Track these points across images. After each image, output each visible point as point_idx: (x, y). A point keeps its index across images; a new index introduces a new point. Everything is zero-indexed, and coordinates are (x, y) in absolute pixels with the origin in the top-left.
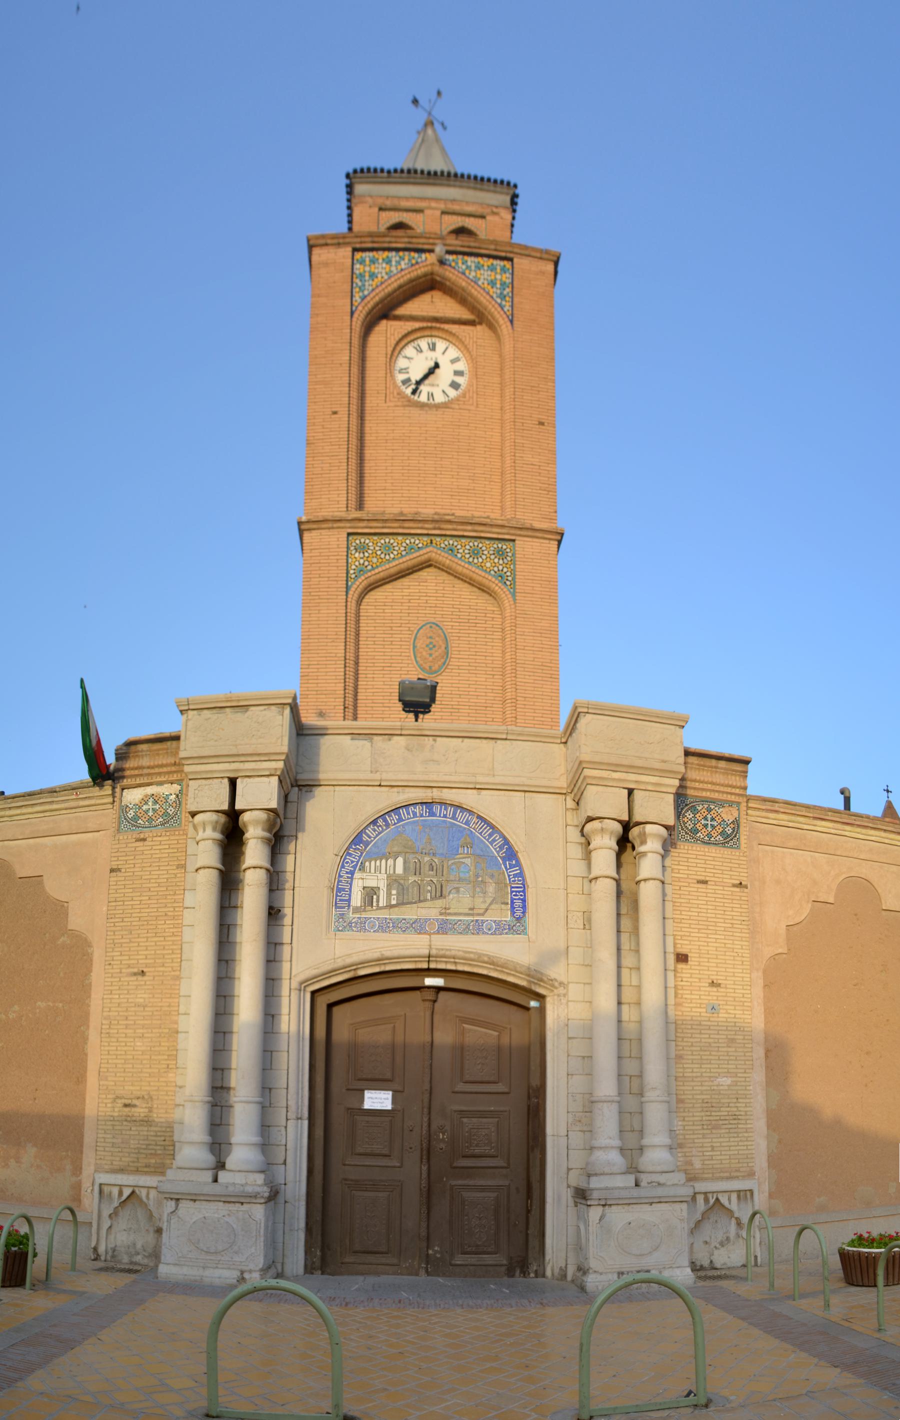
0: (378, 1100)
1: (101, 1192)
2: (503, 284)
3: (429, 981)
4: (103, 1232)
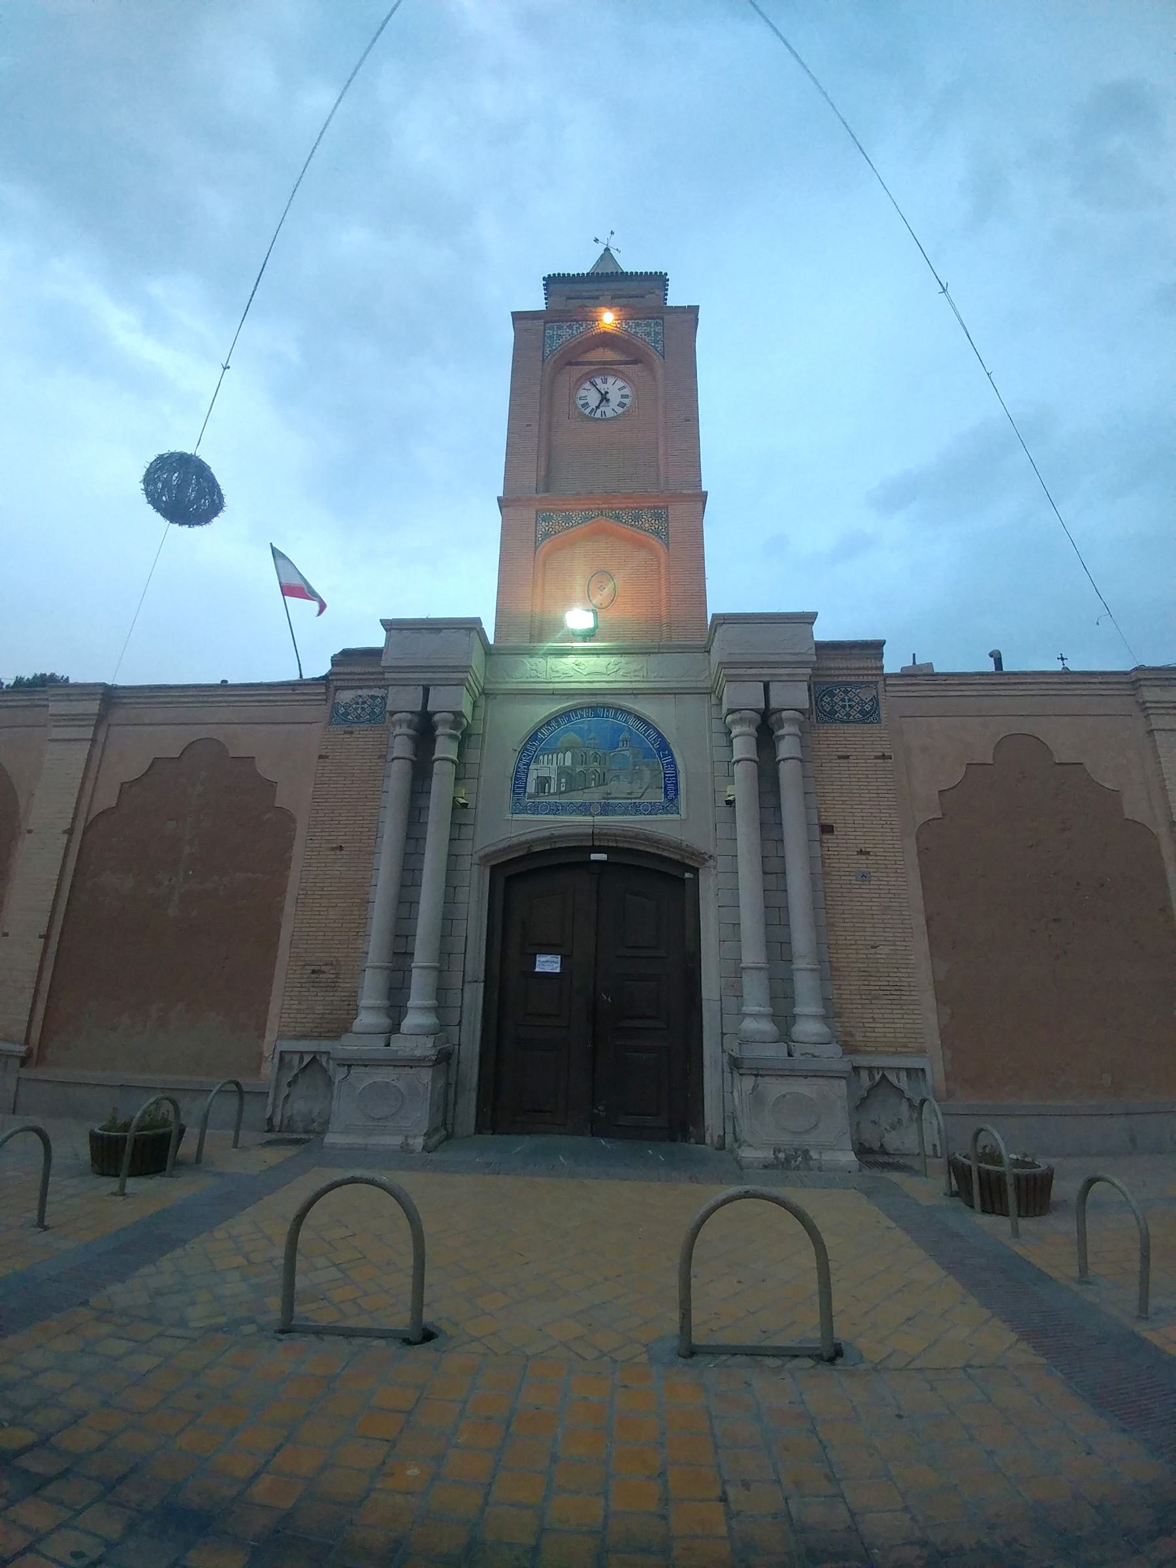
0: (547, 964)
1: (281, 1059)
2: (657, 334)
3: (594, 857)
4: (280, 1103)
